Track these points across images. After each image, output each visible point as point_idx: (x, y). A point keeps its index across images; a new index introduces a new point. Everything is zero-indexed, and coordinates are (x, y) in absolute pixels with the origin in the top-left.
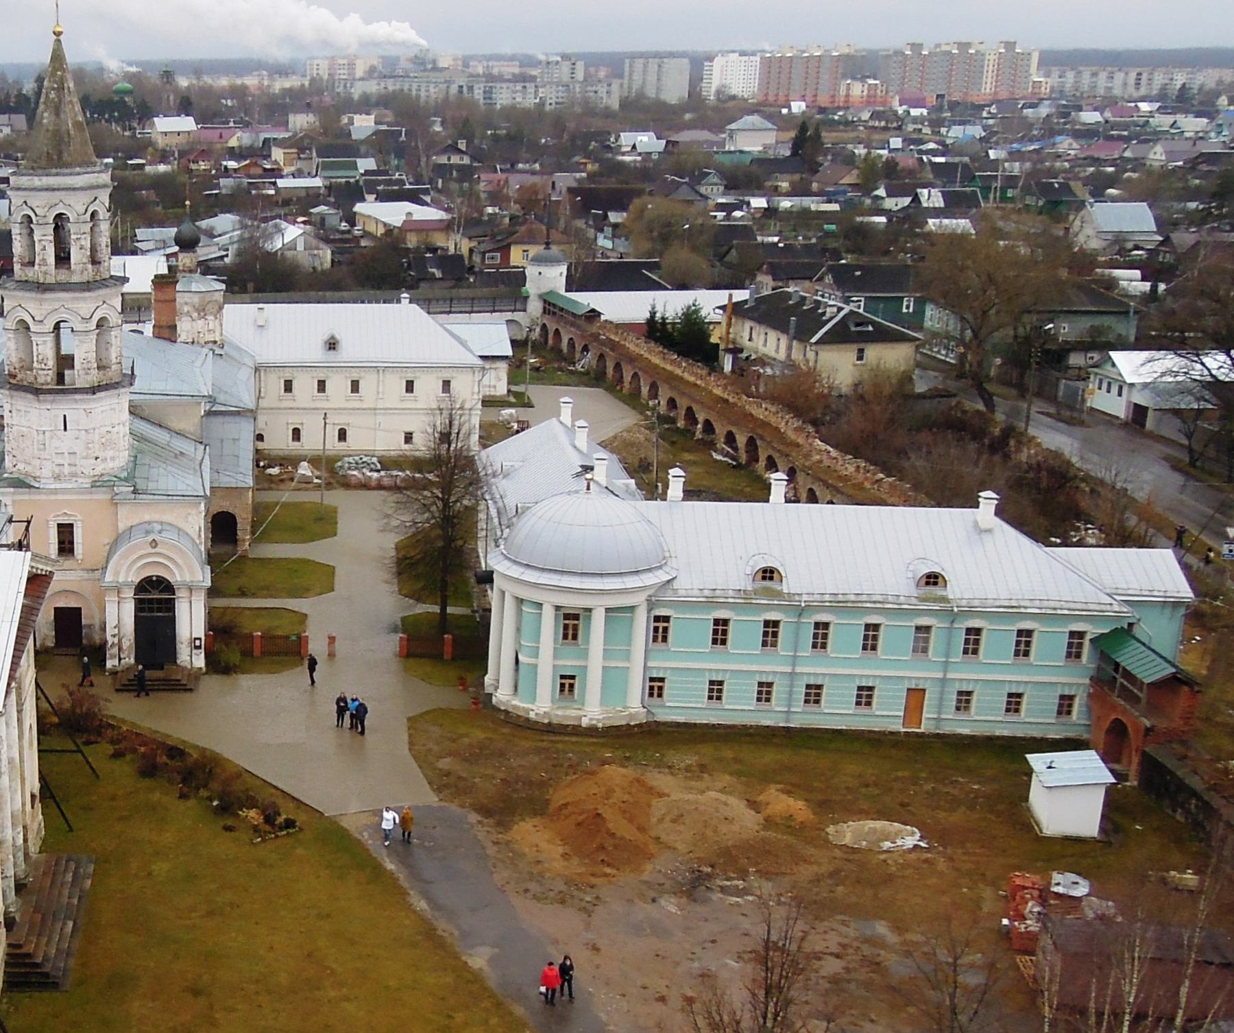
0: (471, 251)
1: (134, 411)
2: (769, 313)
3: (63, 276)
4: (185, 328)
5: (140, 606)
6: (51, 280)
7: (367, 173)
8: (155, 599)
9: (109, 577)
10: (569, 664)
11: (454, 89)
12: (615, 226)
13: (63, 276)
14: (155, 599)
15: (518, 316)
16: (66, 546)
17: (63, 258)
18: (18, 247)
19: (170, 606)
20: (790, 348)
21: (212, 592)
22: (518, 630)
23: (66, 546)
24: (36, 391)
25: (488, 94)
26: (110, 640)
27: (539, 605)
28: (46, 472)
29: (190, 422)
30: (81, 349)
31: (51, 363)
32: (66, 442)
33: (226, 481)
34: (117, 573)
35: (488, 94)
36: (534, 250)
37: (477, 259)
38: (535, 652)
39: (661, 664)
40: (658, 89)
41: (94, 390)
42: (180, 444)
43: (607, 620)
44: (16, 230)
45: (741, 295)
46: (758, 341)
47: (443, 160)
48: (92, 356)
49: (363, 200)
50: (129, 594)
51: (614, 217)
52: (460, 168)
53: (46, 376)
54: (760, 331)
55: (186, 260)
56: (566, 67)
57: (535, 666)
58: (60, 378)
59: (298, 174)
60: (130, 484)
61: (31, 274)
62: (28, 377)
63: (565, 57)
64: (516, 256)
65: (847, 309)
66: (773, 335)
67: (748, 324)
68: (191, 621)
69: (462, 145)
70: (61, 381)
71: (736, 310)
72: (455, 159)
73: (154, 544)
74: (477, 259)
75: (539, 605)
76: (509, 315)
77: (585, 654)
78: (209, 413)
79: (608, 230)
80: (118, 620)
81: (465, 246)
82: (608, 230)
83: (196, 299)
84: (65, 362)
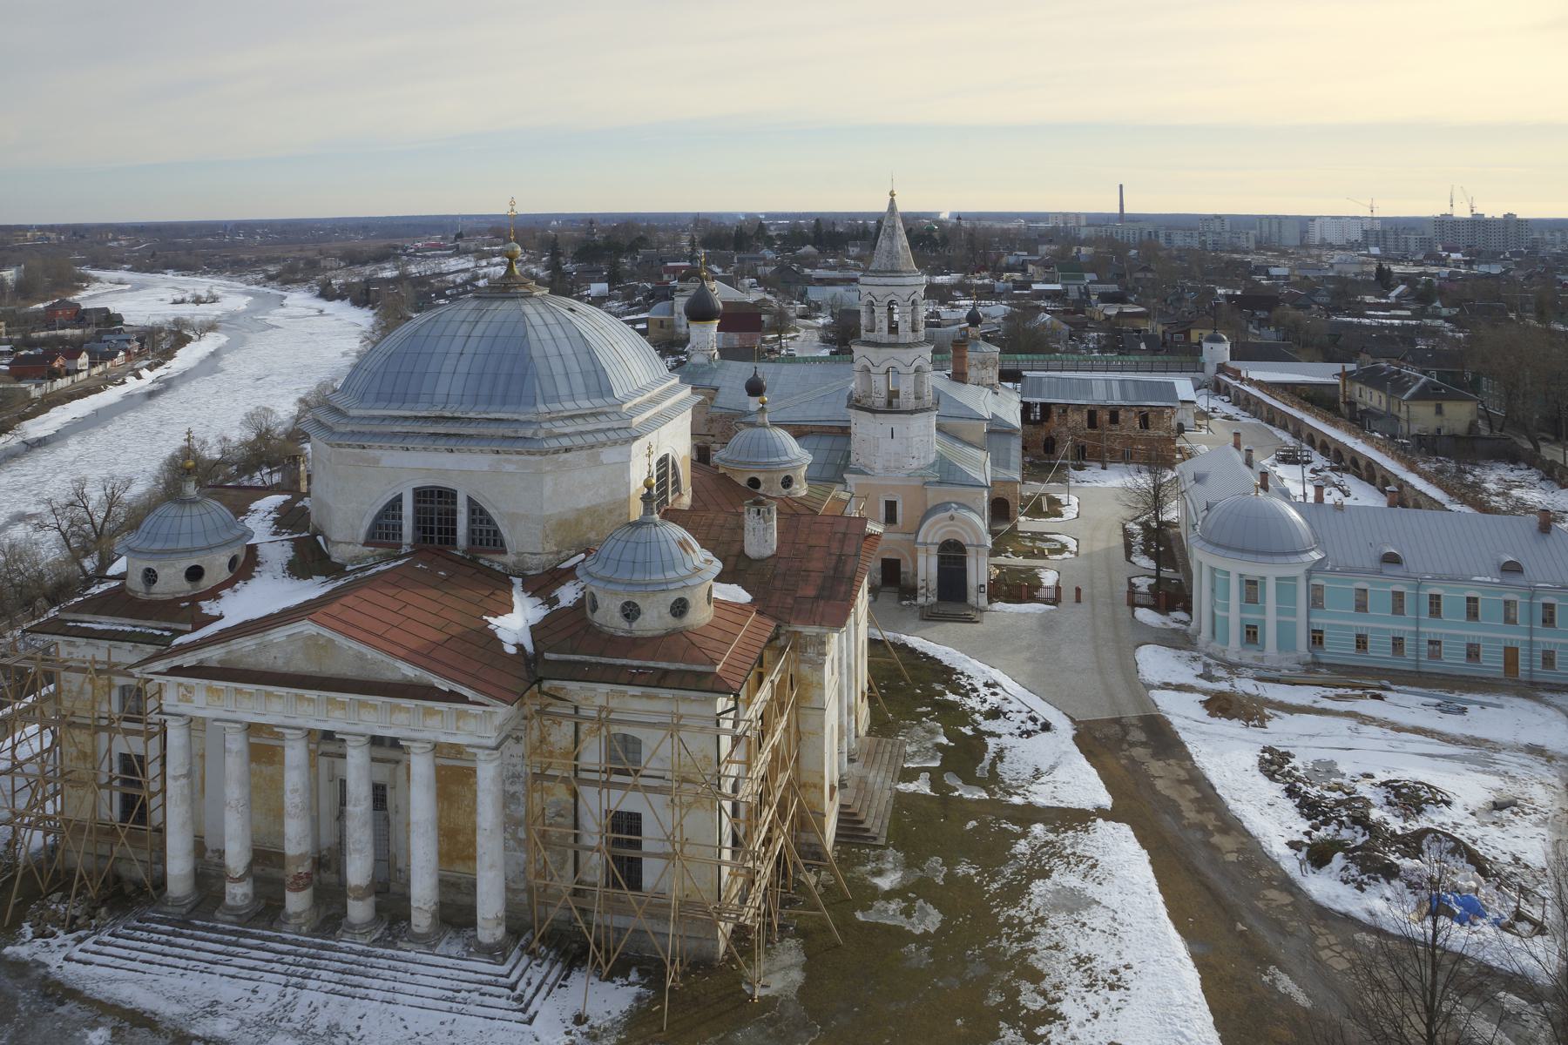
2: (1371, 378)
3: (893, 338)
4: (972, 373)
5: (943, 561)
6: (885, 341)
8: (953, 556)
9: (920, 539)
13: (893, 338)
14: (953, 556)
16: (891, 517)
17: (893, 329)
18: (864, 320)
19: (962, 562)
20: (1388, 403)
21: (994, 553)
23: (891, 517)
24: (874, 411)
26: (920, 584)
28: (878, 467)
30: (906, 386)
31: (884, 394)
33: (1003, 474)
34: (926, 535)
41: (912, 412)
44: (863, 309)
45: (1350, 367)
46: (1366, 397)
50: (934, 550)
53: (880, 402)
54: (1367, 391)
55: (973, 331)
58: (890, 403)
61: (872, 337)
62: (867, 402)
65: (1424, 379)
66: (1376, 394)
67: (1358, 386)
68: (980, 571)
70: (892, 406)
73: (952, 518)
80: (927, 568)
83: (980, 356)
84: (893, 394)
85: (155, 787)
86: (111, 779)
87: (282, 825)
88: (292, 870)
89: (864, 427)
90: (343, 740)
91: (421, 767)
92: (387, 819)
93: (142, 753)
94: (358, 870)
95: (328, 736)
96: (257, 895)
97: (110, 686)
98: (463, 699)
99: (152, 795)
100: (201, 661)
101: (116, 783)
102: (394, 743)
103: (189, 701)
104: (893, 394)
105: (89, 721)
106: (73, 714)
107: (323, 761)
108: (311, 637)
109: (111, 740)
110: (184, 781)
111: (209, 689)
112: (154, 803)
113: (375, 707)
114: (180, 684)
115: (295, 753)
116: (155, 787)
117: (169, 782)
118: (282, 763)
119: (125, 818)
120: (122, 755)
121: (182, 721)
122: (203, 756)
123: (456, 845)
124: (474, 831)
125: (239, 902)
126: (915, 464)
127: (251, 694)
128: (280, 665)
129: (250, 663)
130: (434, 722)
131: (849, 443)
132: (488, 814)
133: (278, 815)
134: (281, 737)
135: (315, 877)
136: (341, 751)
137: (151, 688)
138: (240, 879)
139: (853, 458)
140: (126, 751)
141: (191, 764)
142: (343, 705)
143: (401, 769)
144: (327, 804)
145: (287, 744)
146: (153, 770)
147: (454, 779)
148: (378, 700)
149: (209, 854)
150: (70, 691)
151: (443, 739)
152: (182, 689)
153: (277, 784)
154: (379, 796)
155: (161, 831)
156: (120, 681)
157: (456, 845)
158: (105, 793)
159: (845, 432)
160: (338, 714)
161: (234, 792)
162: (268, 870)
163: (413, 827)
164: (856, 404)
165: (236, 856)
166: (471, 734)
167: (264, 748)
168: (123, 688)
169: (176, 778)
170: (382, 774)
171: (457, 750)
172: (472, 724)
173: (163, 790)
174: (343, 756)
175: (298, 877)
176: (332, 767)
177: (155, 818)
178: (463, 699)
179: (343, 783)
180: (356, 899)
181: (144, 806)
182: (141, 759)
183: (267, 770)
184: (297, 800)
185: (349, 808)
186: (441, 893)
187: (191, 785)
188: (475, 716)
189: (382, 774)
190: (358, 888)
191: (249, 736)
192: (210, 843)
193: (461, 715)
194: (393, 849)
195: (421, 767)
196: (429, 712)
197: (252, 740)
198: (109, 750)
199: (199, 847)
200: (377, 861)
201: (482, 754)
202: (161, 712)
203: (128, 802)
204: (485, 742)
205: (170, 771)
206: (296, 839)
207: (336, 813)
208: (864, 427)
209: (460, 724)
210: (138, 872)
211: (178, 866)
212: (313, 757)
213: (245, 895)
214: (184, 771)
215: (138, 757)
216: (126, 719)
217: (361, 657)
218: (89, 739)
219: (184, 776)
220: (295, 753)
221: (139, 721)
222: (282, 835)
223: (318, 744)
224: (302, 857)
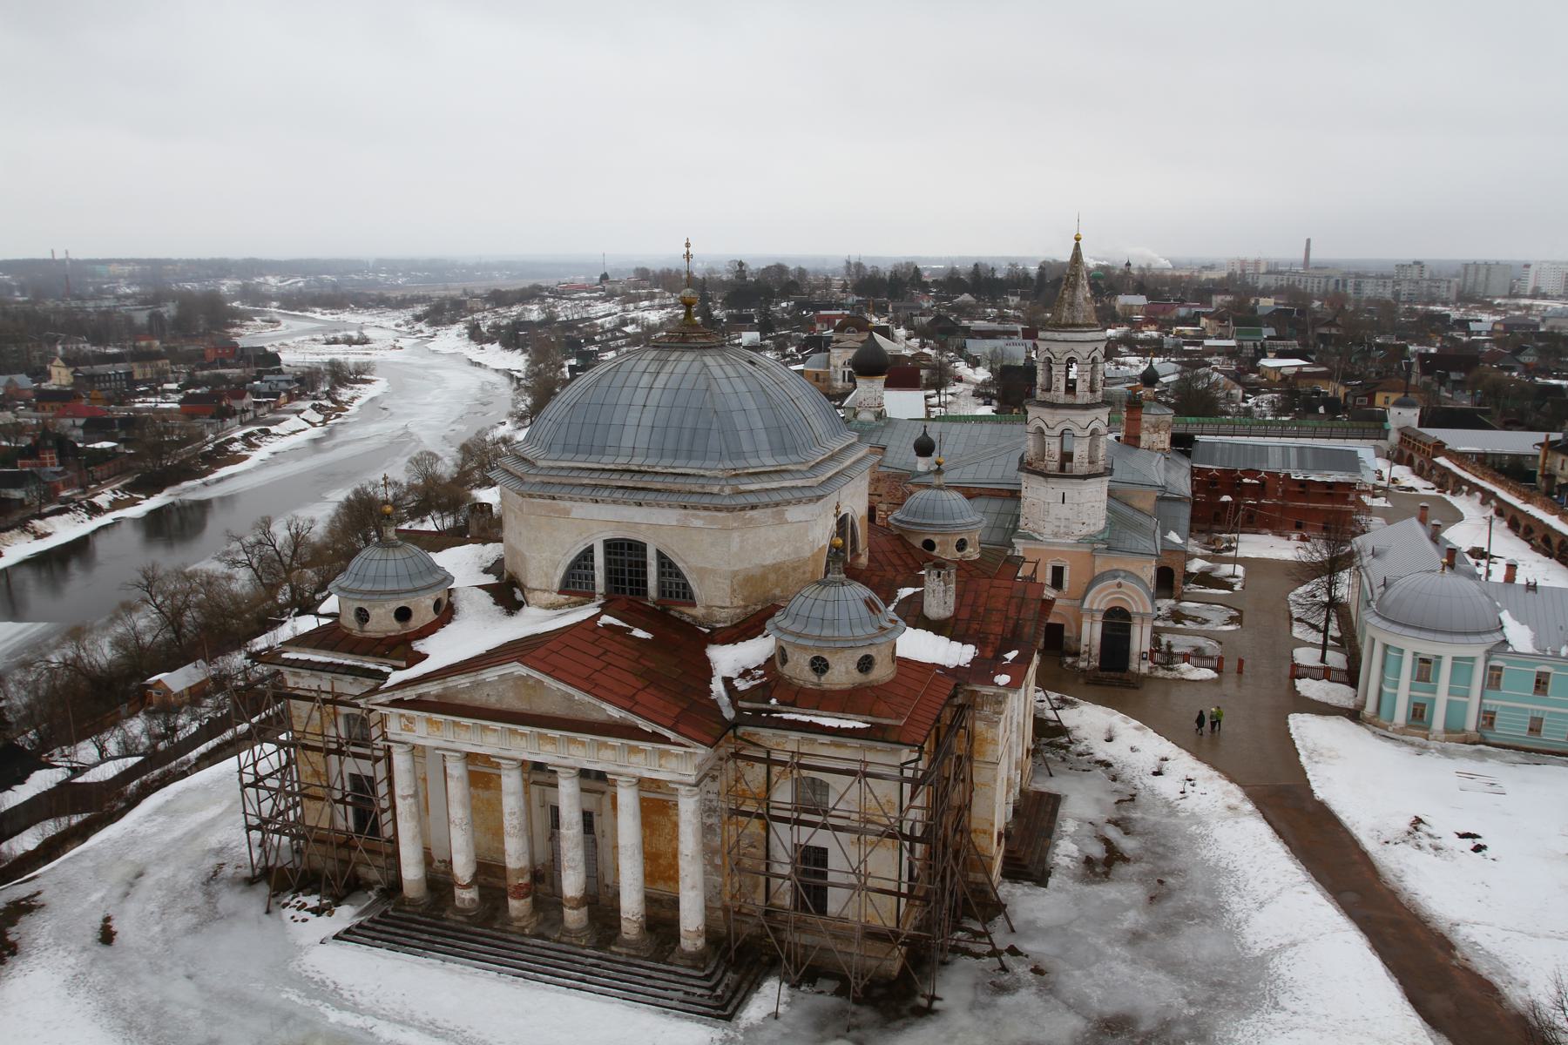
0: (1346, 395)
1: (1111, 494)
4: (1145, 438)
7: (1269, 338)
10: (1421, 695)
11: (1331, 287)
12: (1455, 382)
15: (1381, 443)
22: (1383, 667)
25: (1357, 286)
27: (1402, 651)
29: (1148, 504)
31: (1057, 457)
32: (1064, 511)
35: (1357, 286)
36: (1394, 397)
37: (1350, 401)
38: (1396, 685)
39: (1492, 703)
40: (1486, 287)
42: (1140, 518)
43: (1453, 665)
47: (1324, 330)
48: (1086, 454)
49: (1265, 357)
51: (1454, 376)
52: (1337, 338)
56: (1416, 270)
57: (1395, 695)
58: (1062, 468)
59: (1220, 337)
60: (1109, 542)
62: (1041, 466)
63: (1417, 263)
64: (1379, 399)
69: (1339, 321)
70: (1065, 469)
71: (1549, 446)
72: (1334, 331)
74: (1350, 401)
75: (1402, 651)
76: (1374, 442)
77: (1434, 691)
78: (1161, 499)
79: (1449, 385)
81: (1342, 391)
82: (1449, 385)
83: (1153, 419)
84: (1067, 457)
89: (1036, 493)
104: (1067, 457)
126: (1085, 531)
131: (1018, 507)
139: (1022, 522)
159: (1015, 495)
164: (1026, 467)
208: (1036, 493)
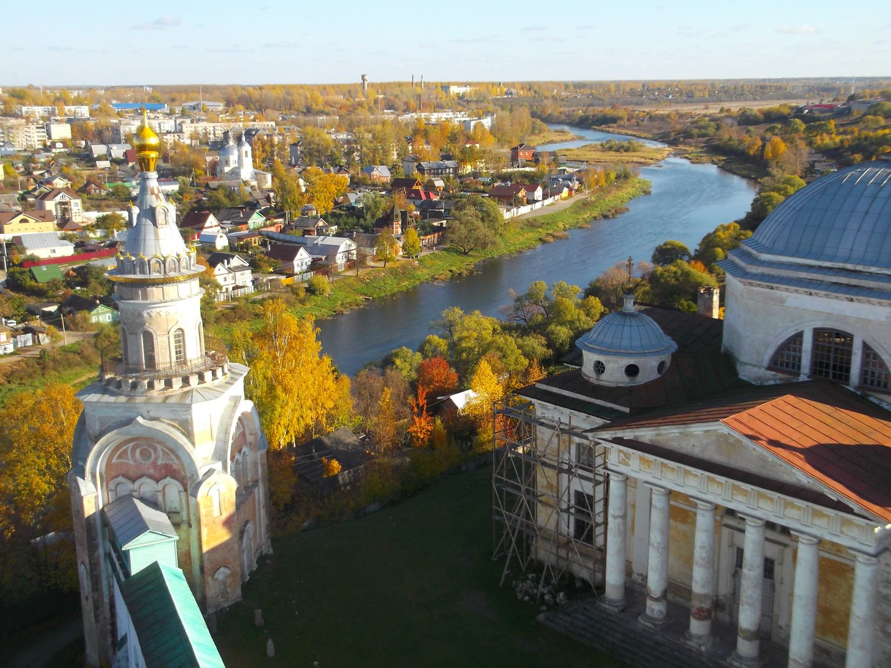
85: (599, 519)
86: (569, 508)
87: (691, 569)
88: (696, 604)
90: (743, 519)
91: (806, 554)
92: (773, 586)
93: (591, 493)
94: (747, 618)
95: (731, 512)
96: (668, 615)
97: (570, 442)
98: (849, 511)
99: (598, 525)
100: (637, 437)
101: (572, 511)
102: (785, 530)
103: (627, 464)
105: (556, 464)
106: (544, 456)
107: (726, 531)
108: (723, 435)
109: (569, 481)
110: (619, 520)
111: (642, 459)
112: (599, 530)
113: (771, 500)
114: (620, 451)
115: (704, 520)
116: (599, 519)
117: (610, 519)
118: (693, 524)
119: (578, 535)
120: (577, 492)
121: (621, 478)
122: (634, 506)
123: (831, 619)
124: (847, 615)
125: (655, 615)
127: (673, 469)
128: (696, 452)
129: (674, 445)
130: (822, 522)
132: (860, 605)
133: (689, 560)
134: (695, 506)
135: (713, 614)
136: (740, 526)
137: (599, 450)
138: (656, 600)
140: (580, 490)
141: (626, 509)
142: (745, 493)
143: (788, 553)
144: (727, 560)
145: (699, 512)
146: (599, 507)
147: (834, 571)
148: (775, 495)
149: (635, 576)
150: (542, 439)
151: (828, 537)
152: (622, 455)
153: (689, 539)
154: (769, 568)
155: (603, 550)
156: (577, 440)
157: (831, 619)
158: (565, 515)
160: (740, 498)
161: (656, 537)
162: (678, 599)
163: (796, 599)
165: (655, 583)
166: (853, 538)
167: (680, 510)
168: (579, 445)
169: (615, 517)
170: (772, 551)
171: (837, 548)
172: (855, 532)
173: (606, 523)
174: (743, 531)
175: (701, 610)
176: (732, 537)
177: (599, 541)
178: (849, 511)
179: (740, 552)
180: (745, 638)
181: (591, 531)
182: (591, 498)
183: (682, 527)
184: (704, 555)
185: (745, 570)
186: (815, 654)
187: (625, 524)
188: (858, 526)
189: (772, 551)
190: (745, 631)
191: (669, 500)
192: (636, 568)
193: (844, 522)
194: (776, 609)
195: (806, 554)
196: (816, 514)
197: (672, 503)
198: (569, 488)
199: (628, 571)
200: (763, 615)
201: (861, 558)
202: (606, 468)
203: (581, 527)
204: (864, 548)
205: (611, 511)
206: (699, 581)
207: (733, 571)
209: (845, 529)
210: (584, 574)
211: (613, 577)
212: (718, 526)
213: (661, 612)
214: (621, 514)
215: (588, 496)
216: (581, 468)
217: (762, 459)
218: (555, 475)
219: (621, 517)
220: (704, 520)
221: (591, 471)
222: (690, 577)
223: (722, 516)
224: (705, 596)
